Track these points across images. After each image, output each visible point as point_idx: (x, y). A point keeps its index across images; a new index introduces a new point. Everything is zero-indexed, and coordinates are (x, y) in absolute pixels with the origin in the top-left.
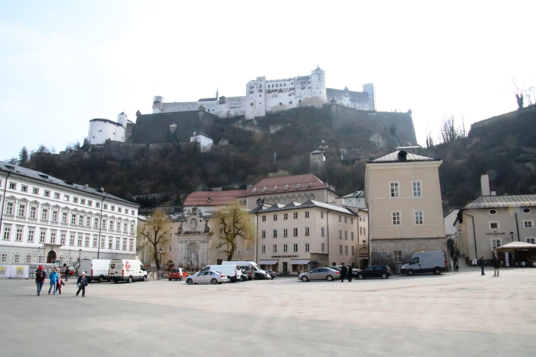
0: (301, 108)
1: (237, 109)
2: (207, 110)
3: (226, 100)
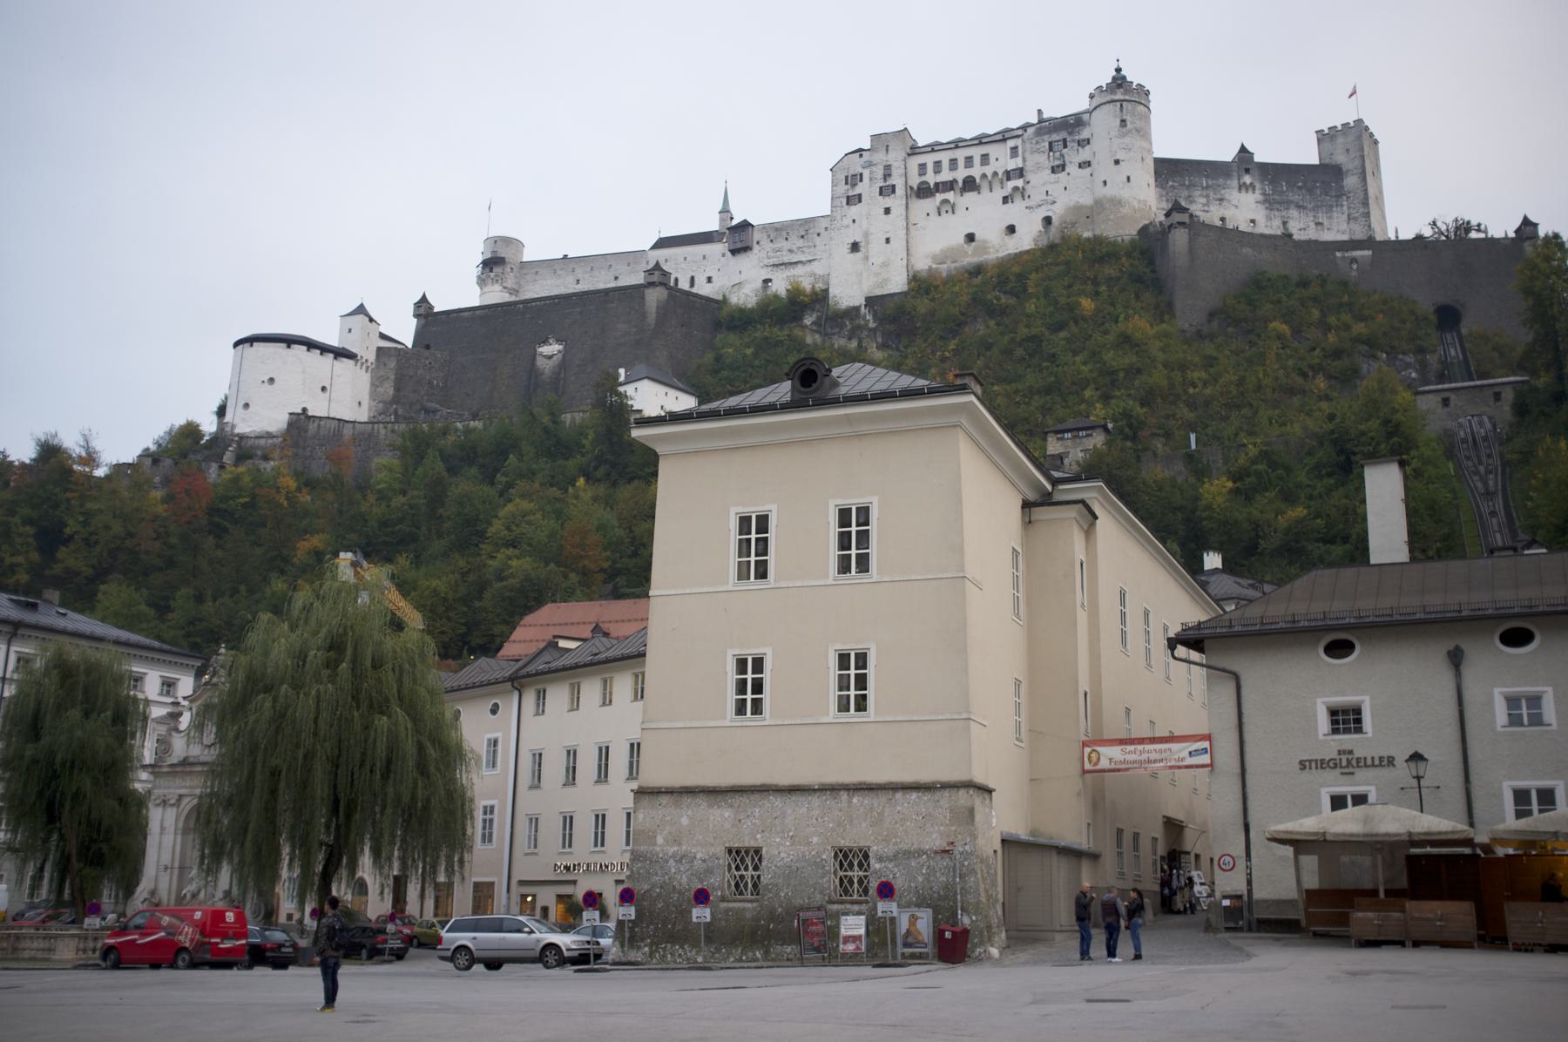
0: (1052, 247)
1: (799, 271)
2: (684, 285)
3: (757, 236)
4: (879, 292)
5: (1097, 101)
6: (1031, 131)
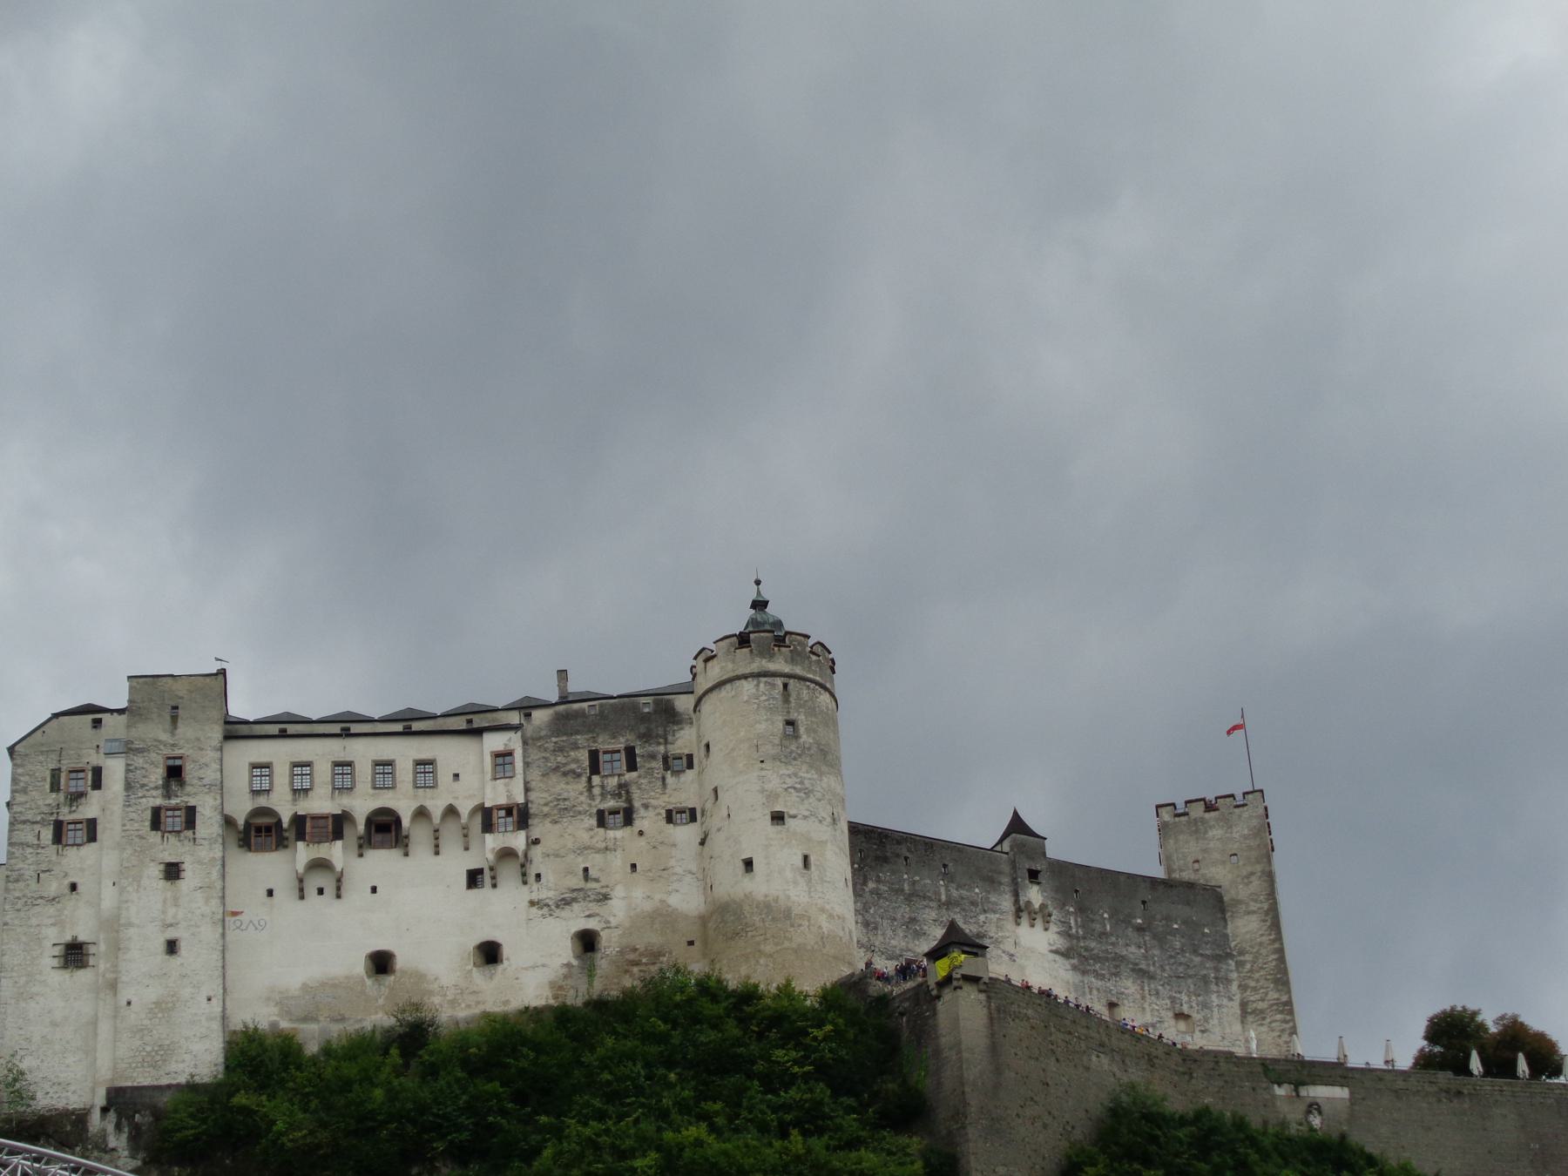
4: (143, 1078)
5: (715, 672)
6: (540, 716)
